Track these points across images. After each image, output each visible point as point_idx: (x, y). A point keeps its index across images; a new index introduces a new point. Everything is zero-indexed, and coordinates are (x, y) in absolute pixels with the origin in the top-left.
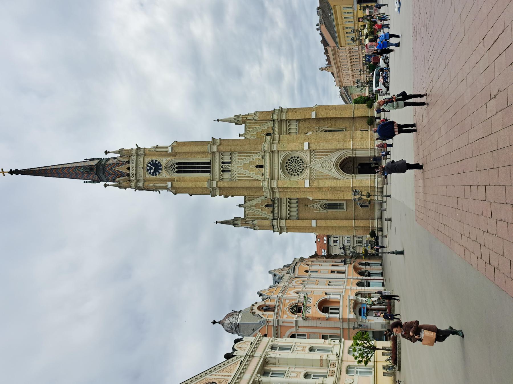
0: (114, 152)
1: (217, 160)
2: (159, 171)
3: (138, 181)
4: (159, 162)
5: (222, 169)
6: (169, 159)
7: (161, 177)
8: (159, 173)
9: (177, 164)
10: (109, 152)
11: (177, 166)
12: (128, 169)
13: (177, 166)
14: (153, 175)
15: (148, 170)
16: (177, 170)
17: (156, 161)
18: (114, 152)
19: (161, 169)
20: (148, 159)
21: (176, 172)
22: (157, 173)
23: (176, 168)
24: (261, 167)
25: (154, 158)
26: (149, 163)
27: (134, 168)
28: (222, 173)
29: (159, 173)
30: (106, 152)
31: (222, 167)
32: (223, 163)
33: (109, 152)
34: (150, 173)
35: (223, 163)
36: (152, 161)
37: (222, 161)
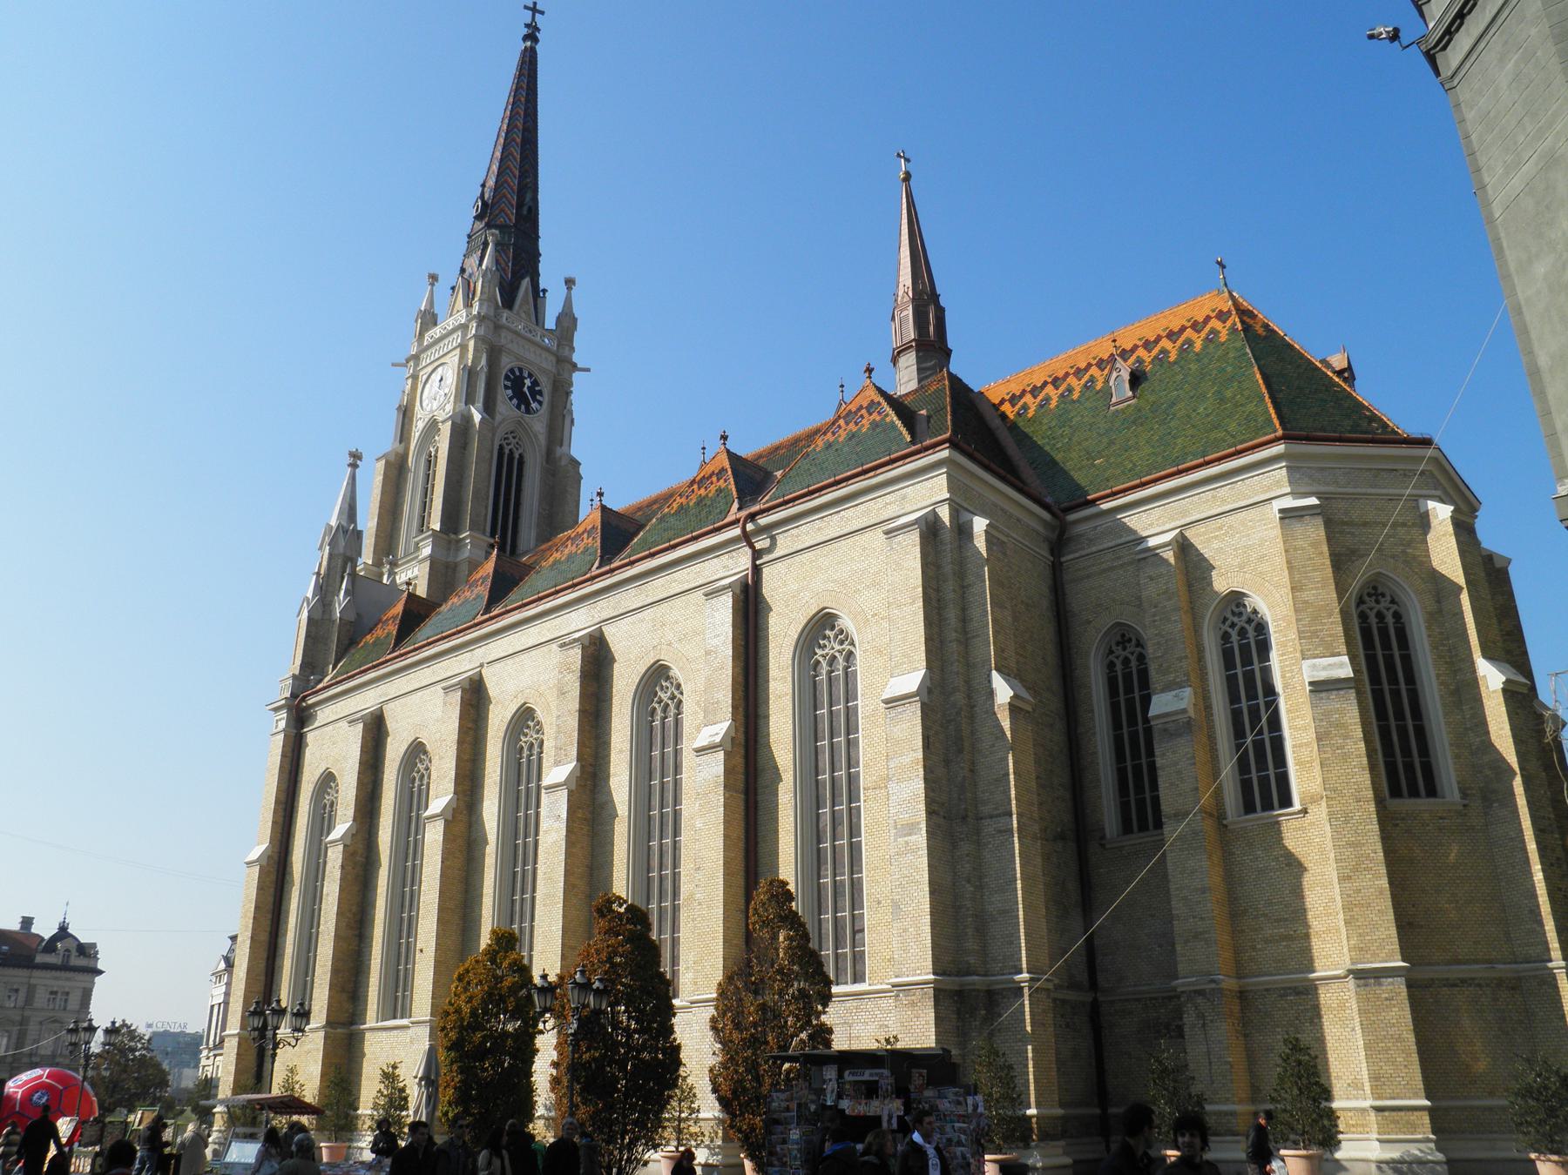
0: (568, 302)
2: (515, 401)
6: (542, 439)
7: (499, 398)
10: (569, 289)
14: (507, 378)
17: (540, 403)
18: (568, 302)
19: (518, 407)
20: (545, 386)
21: (501, 448)
22: (510, 392)
25: (546, 399)
30: (570, 283)
33: (569, 289)
34: (512, 371)
36: (540, 393)
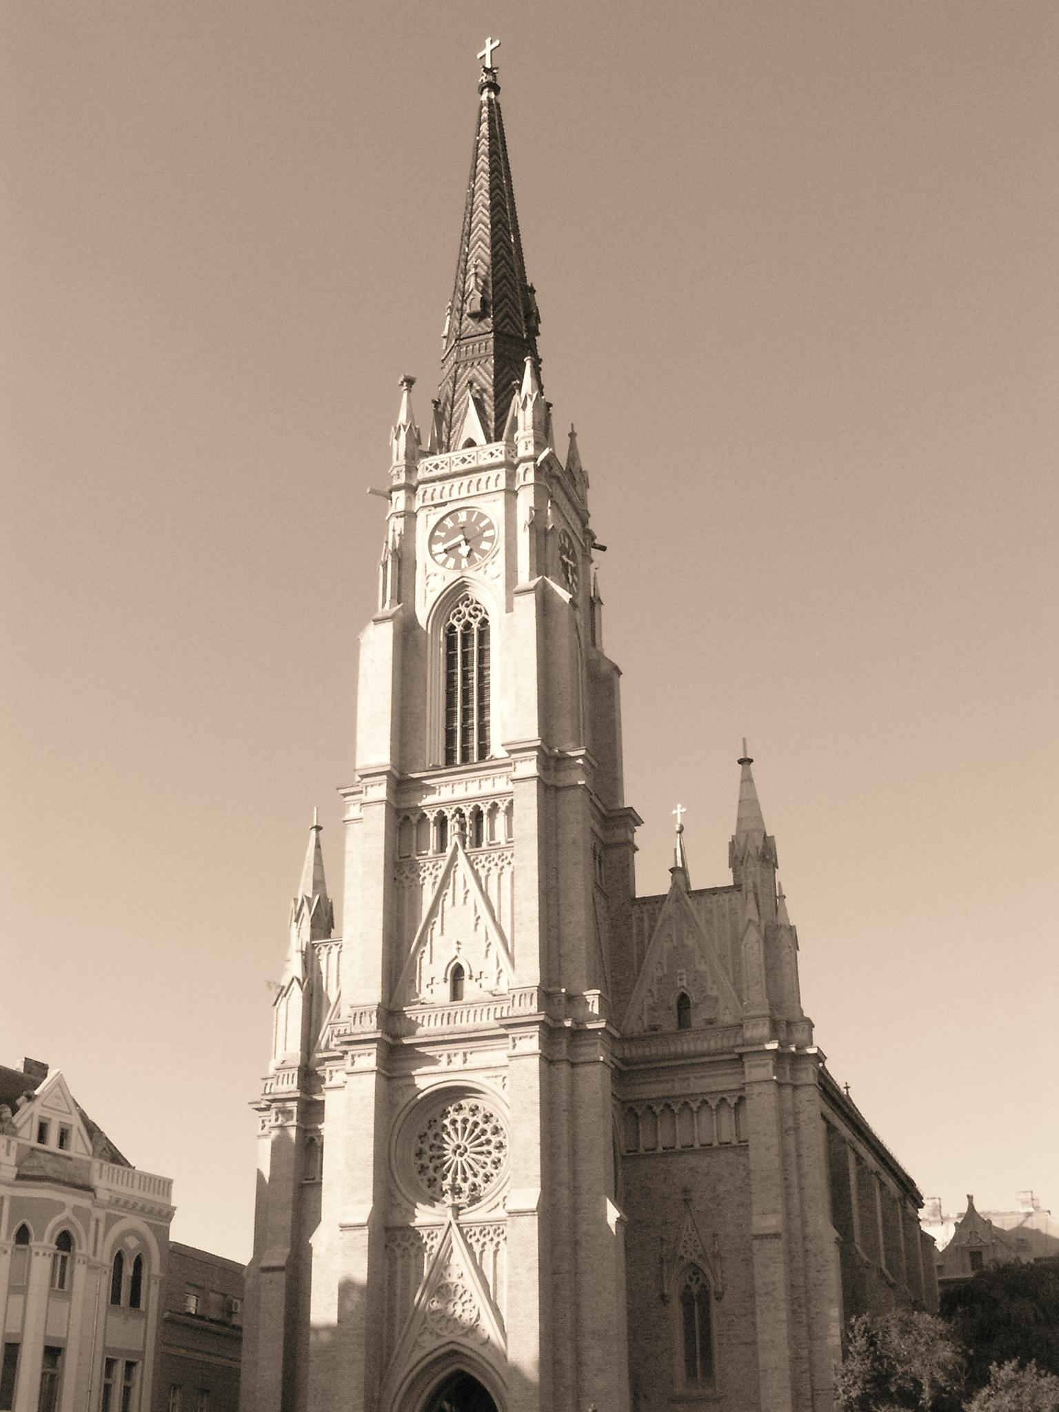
1: (487, 788)
3: (411, 490)
4: (483, 553)
5: (449, 815)
8: (444, 564)
9: (484, 622)
11: (475, 626)
12: (470, 443)
13: (475, 626)
15: (455, 520)
16: (459, 629)
17: (491, 539)
23: (468, 626)
24: (456, 994)
26: (482, 517)
27: (466, 466)
28: (431, 816)
29: (444, 564)
31: (459, 811)
32: (478, 815)
35: (478, 815)
36: (490, 526)
37: (485, 809)
